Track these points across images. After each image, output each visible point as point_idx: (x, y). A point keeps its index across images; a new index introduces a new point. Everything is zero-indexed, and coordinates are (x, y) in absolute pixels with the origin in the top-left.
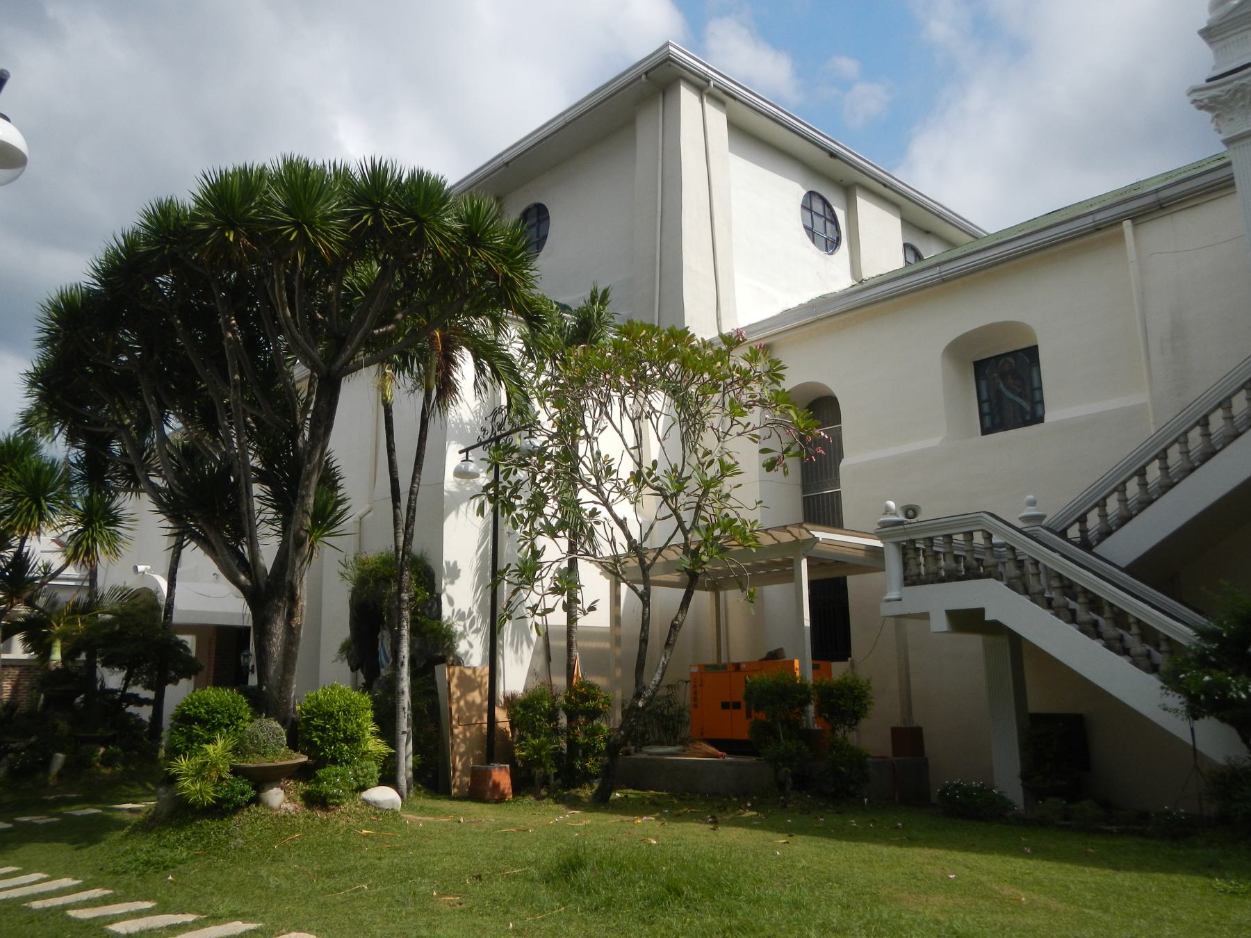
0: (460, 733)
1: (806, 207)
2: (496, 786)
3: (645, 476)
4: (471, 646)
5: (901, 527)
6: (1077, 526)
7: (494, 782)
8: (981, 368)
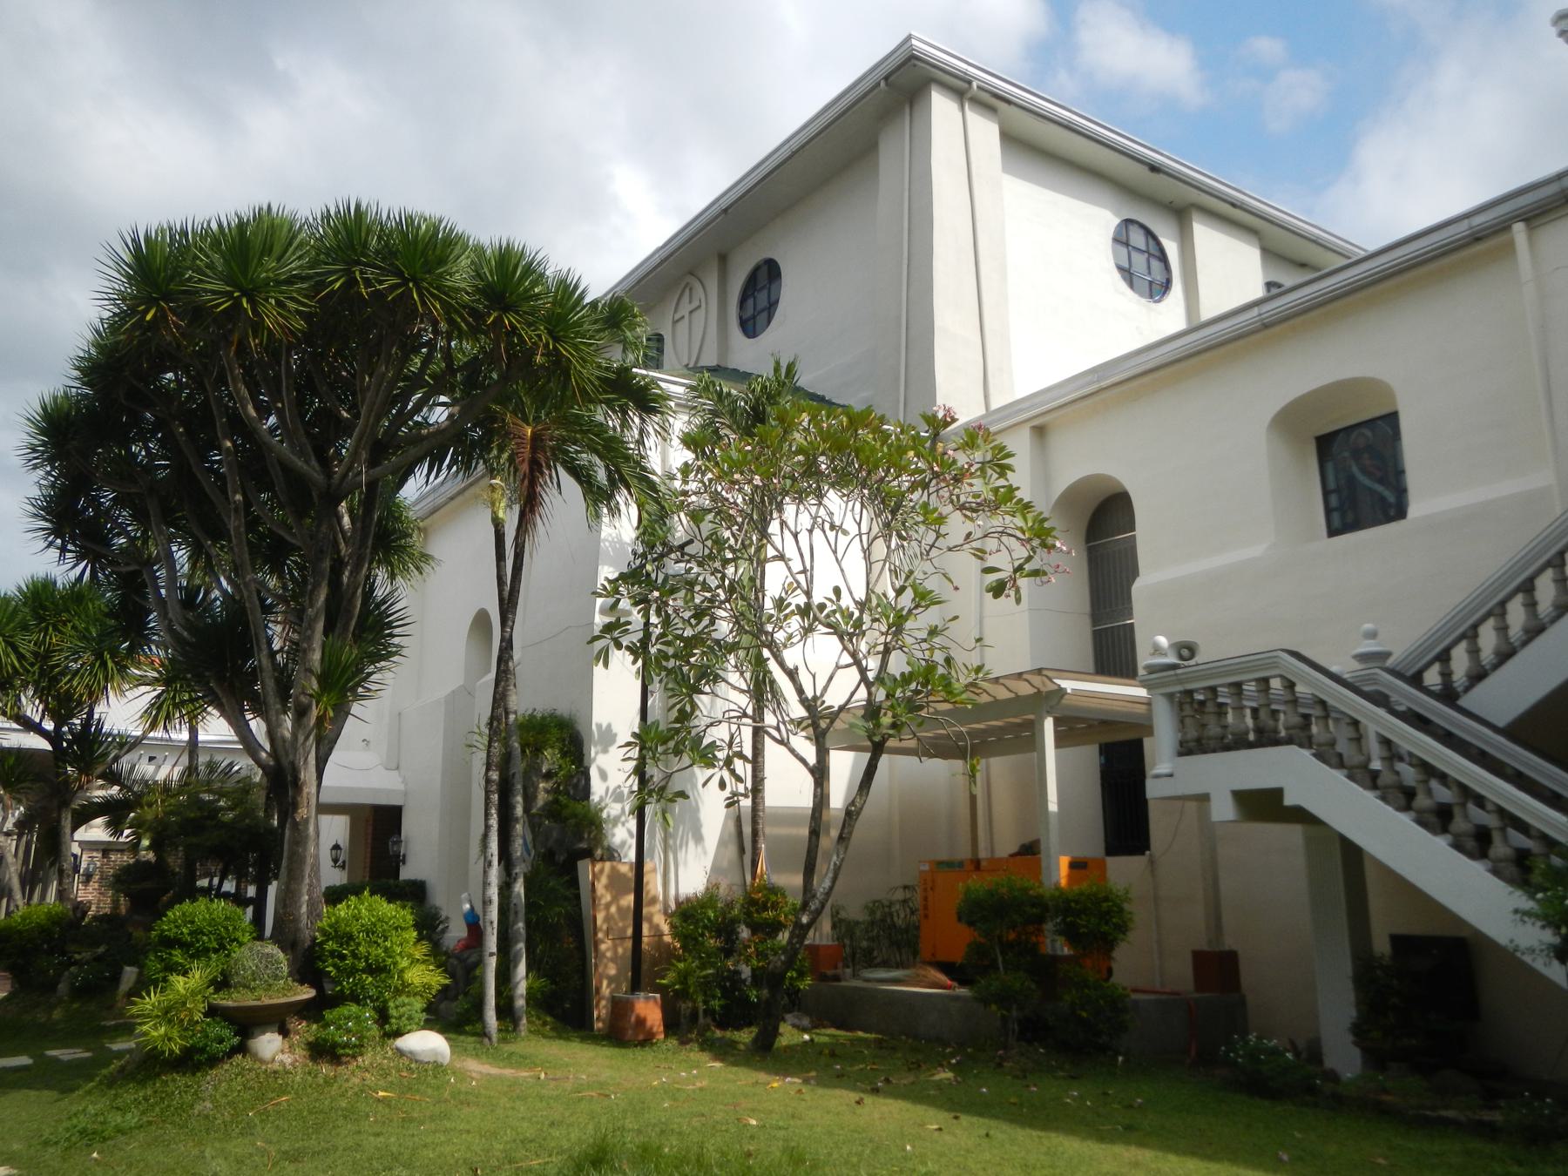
0: (608, 949)
1: (1120, 240)
2: (641, 1022)
3: (815, 609)
5: (1172, 672)
6: (1436, 667)
7: (638, 1017)
8: (1325, 444)
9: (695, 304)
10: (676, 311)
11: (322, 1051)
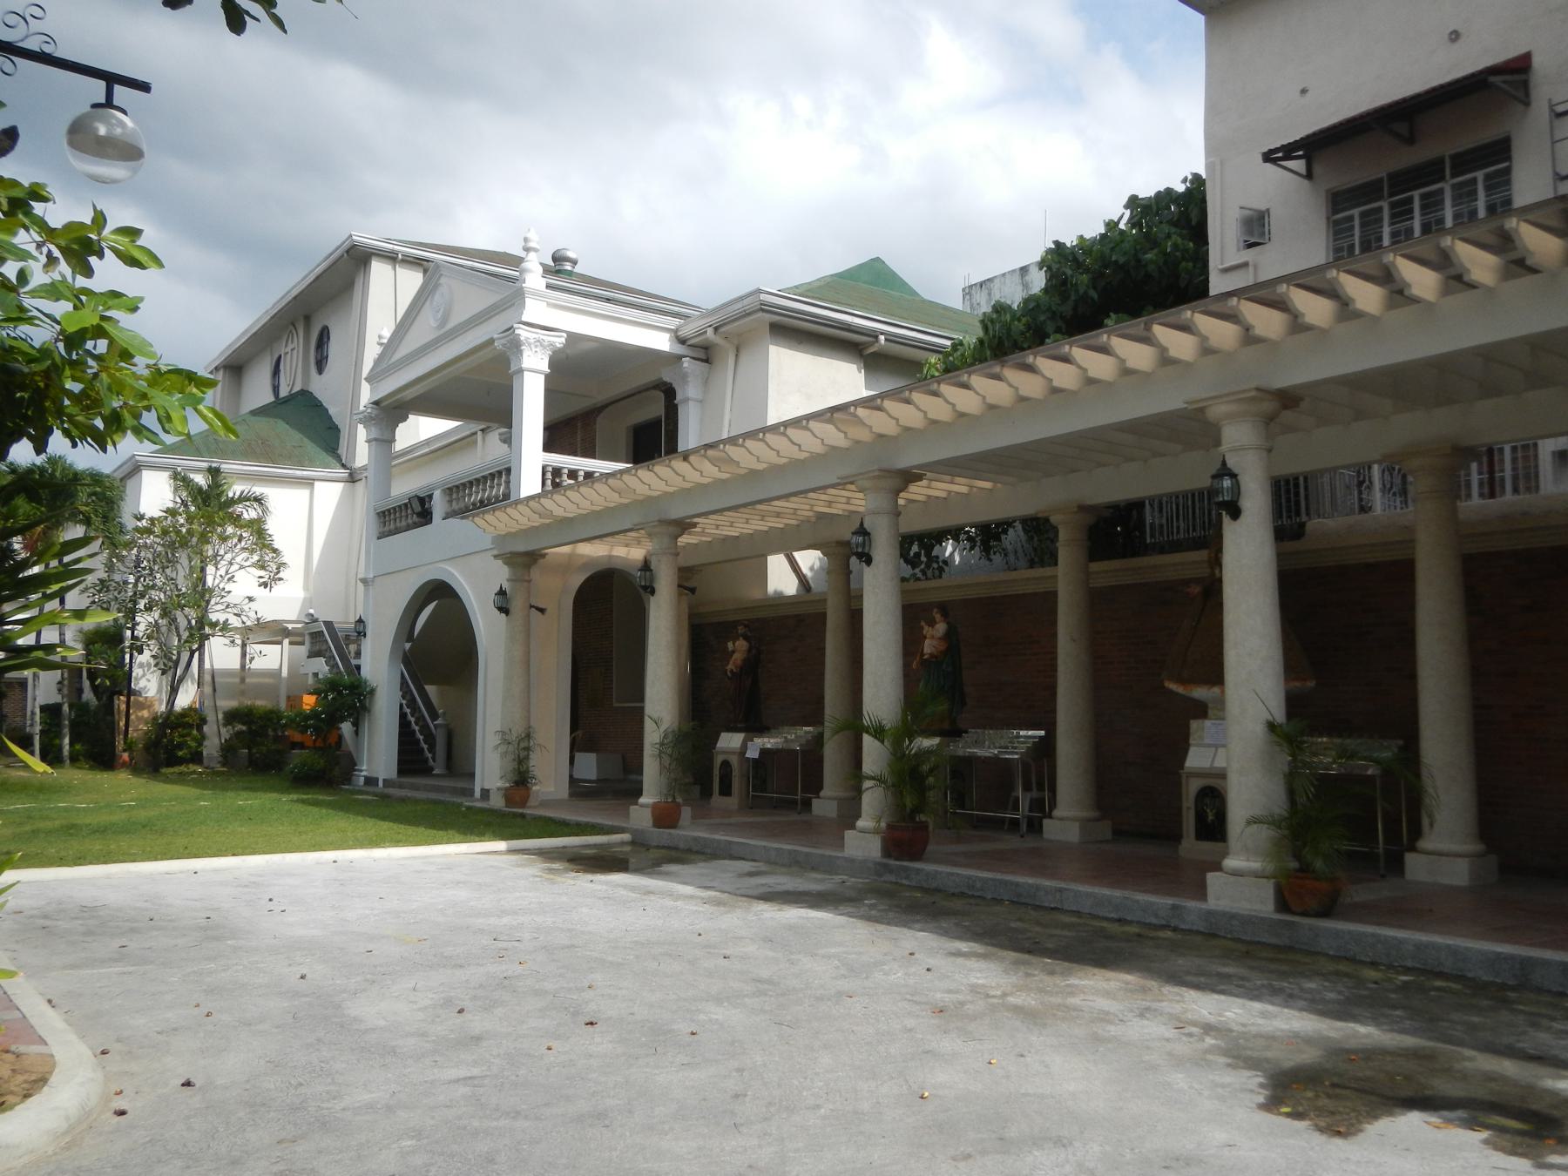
10: (286, 346)
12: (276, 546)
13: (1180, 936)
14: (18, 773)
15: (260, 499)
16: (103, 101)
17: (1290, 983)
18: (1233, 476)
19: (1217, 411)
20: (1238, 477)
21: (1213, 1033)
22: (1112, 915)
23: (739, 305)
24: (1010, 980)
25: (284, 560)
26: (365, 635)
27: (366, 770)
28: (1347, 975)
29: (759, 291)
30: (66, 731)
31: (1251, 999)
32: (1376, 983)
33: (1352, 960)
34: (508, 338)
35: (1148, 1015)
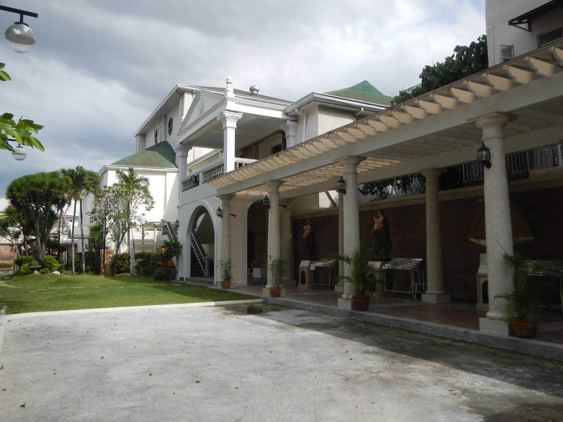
4: (112, 244)
9: (161, 126)
10: (159, 126)
11: (42, 273)
12: (151, 196)
13: (467, 345)
14: (67, 276)
15: (147, 180)
16: (19, 21)
17: (510, 369)
18: (487, 150)
19: (480, 123)
20: (490, 151)
21: (466, 394)
22: (440, 335)
23: (307, 99)
24: (384, 365)
25: (154, 200)
26: (179, 227)
27: (180, 275)
28: (538, 365)
29: (313, 93)
30: (84, 262)
31: (489, 377)
32: (550, 370)
33: (542, 358)
34: (221, 116)
35: (439, 384)
